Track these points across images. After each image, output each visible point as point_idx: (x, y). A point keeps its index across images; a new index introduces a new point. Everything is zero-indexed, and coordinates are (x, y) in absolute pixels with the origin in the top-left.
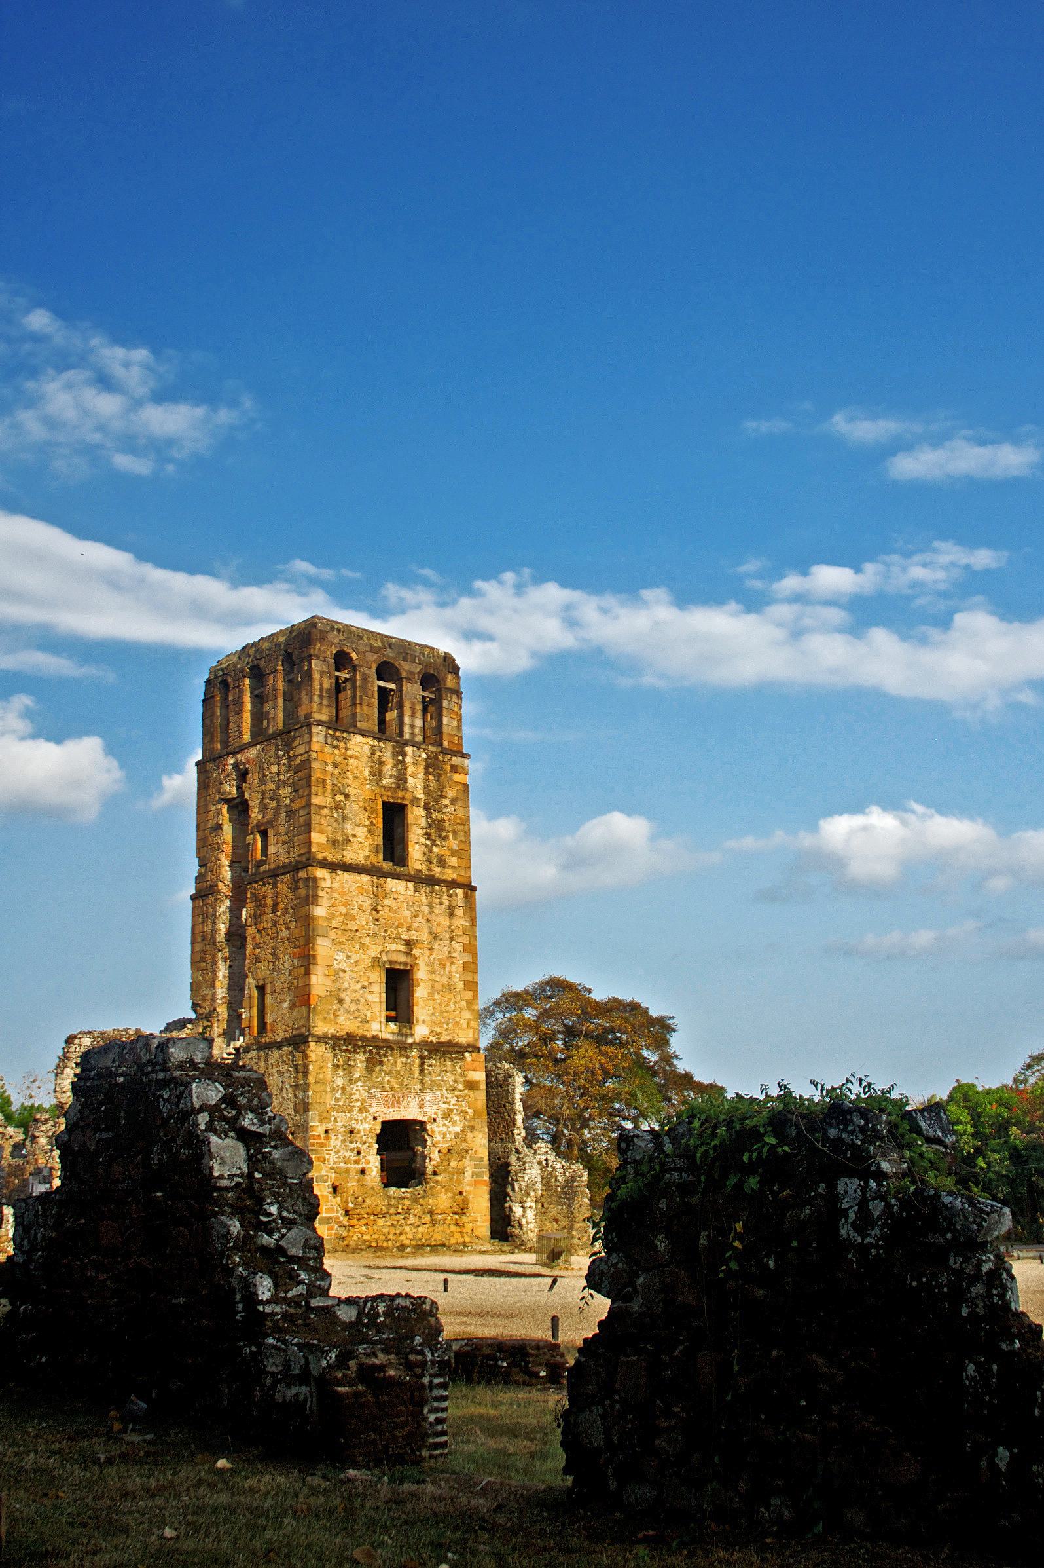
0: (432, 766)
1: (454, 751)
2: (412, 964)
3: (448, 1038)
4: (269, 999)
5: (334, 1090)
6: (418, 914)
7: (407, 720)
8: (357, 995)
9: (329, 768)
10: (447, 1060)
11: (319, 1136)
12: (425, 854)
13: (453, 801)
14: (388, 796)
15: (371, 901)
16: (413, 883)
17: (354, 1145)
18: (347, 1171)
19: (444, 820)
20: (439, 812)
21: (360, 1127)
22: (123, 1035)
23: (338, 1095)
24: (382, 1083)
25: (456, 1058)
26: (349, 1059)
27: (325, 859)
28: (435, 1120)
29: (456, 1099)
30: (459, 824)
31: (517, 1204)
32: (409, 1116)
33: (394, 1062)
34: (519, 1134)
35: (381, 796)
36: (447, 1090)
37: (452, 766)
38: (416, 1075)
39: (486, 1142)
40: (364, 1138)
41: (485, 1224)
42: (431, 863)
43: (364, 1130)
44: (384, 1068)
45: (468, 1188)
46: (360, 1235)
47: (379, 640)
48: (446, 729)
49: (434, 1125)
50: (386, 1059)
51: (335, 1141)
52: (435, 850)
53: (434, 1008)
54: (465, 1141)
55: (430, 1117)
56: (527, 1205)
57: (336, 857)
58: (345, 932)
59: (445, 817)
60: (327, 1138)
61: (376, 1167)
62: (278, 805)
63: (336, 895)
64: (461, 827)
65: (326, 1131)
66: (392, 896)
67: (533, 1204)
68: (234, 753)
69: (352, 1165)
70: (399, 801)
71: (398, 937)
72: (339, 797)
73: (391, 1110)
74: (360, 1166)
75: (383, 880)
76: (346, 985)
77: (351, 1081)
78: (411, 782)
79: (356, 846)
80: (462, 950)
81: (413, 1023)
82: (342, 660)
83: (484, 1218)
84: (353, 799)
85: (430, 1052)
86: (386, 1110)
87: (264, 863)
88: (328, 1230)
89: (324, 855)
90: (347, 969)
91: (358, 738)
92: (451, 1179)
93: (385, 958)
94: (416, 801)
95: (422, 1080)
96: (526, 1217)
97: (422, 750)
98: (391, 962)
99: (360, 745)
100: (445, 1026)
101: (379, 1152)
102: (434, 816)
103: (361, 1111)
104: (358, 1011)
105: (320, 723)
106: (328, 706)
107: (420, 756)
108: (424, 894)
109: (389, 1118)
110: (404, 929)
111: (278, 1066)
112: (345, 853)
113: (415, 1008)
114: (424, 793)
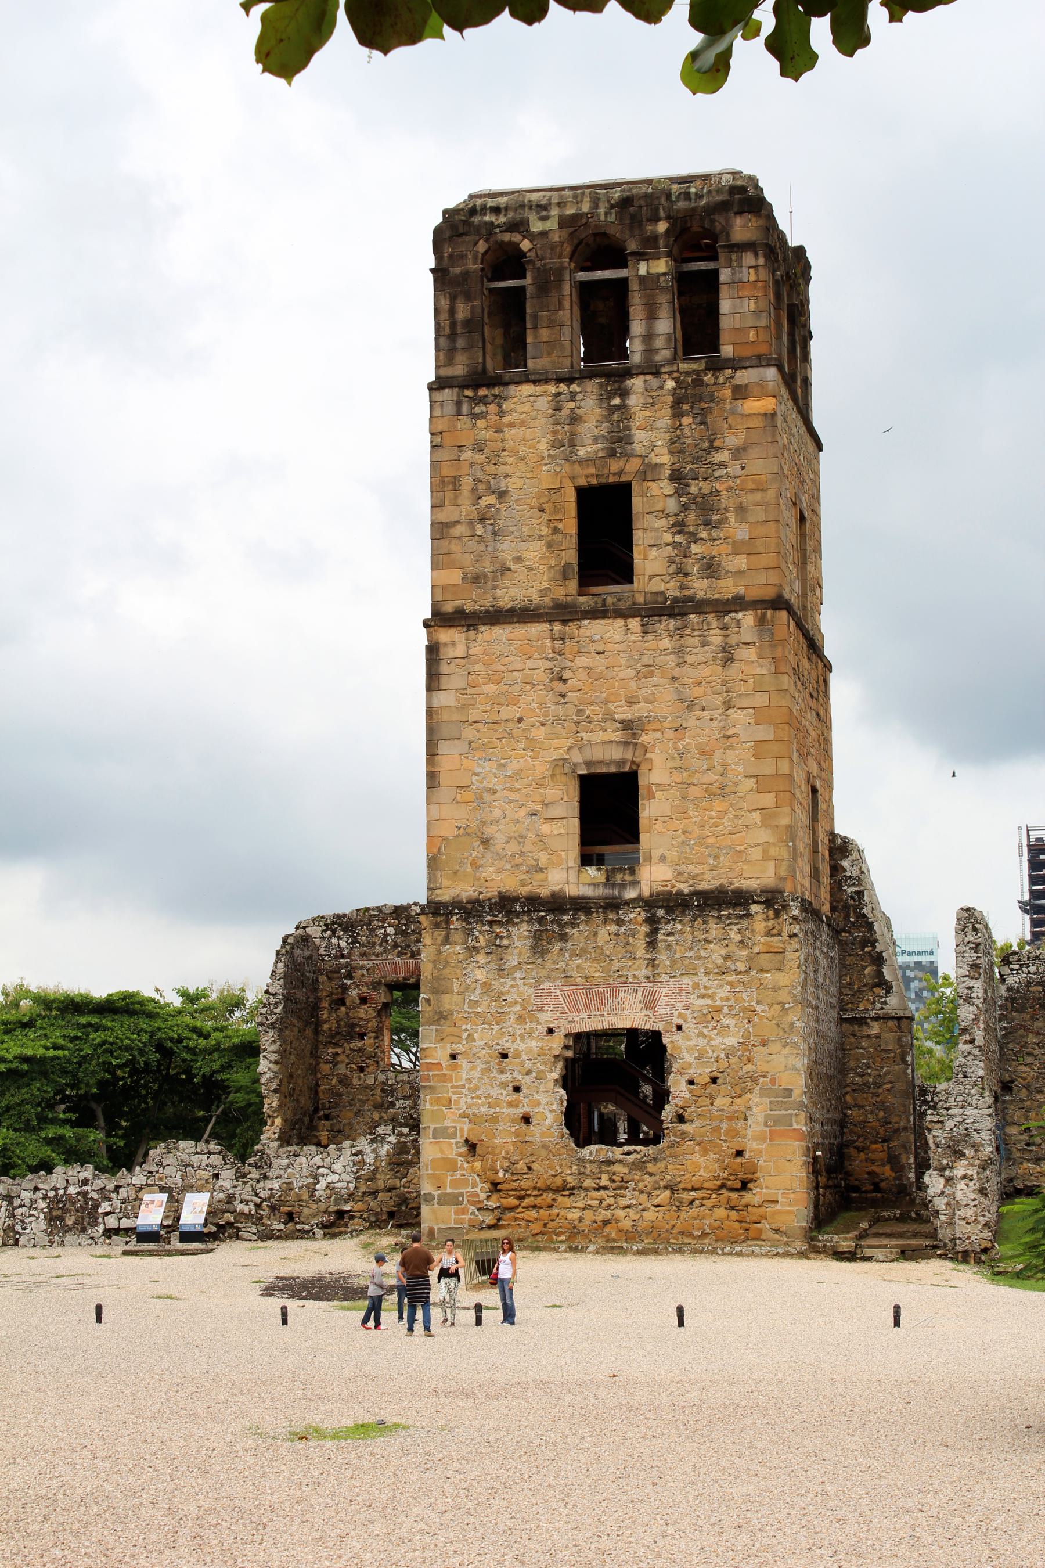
1: (742, 359)
2: (637, 760)
6: (652, 672)
7: (637, 327)
9: (467, 455)
10: (711, 920)
11: (440, 1064)
13: (738, 452)
14: (587, 476)
15: (550, 665)
16: (638, 619)
18: (494, 1119)
20: (705, 479)
21: (522, 1047)
22: (375, 916)
25: (729, 916)
28: (679, 1028)
29: (728, 987)
30: (752, 491)
31: (935, 1173)
32: (623, 1022)
34: (972, 1042)
35: (572, 478)
36: (706, 974)
38: (641, 951)
40: (528, 1065)
41: (795, 1209)
42: (686, 575)
43: (530, 1051)
44: (569, 945)
45: (755, 1145)
46: (523, 1223)
47: (587, 199)
48: (725, 323)
49: (679, 1037)
50: (574, 931)
51: (465, 1070)
53: (685, 832)
56: (959, 1172)
57: (481, 602)
58: (495, 726)
59: (717, 486)
60: (454, 1068)
61: (552, 1111)
63: (478, 667)
64: (758, 497)
65: (453, 1057)
66: (592, 649)
69: (504, 1110)
70: (611, 480)
71: (609, 717)
73: (584, 1015)
74: (520, 1111)
75: (571, 628)
76: (497, 813)
80: (752, 721)
83: (792, 1196)
84: (516, 497)
85: (669, 910)
88: (456, 1213)
89: (457, 603)
90: (498, 788)
91: (527, 389)
92: (716, 1130)
93: (577, 757)
94: (649, 472)
95: (654, 960)
96: (954, 1193)
97: (667, 376)
98: (588, 764)
100: (712, 862)
102: (693, 489)
103: (521, 1019)
104: (522, 854)
106: (469, 348)
107: (661, 388)
108: (665, 634)
109: (578, 1028)
110: (623, 703)
112: (499, 593)
114: (671, 453)
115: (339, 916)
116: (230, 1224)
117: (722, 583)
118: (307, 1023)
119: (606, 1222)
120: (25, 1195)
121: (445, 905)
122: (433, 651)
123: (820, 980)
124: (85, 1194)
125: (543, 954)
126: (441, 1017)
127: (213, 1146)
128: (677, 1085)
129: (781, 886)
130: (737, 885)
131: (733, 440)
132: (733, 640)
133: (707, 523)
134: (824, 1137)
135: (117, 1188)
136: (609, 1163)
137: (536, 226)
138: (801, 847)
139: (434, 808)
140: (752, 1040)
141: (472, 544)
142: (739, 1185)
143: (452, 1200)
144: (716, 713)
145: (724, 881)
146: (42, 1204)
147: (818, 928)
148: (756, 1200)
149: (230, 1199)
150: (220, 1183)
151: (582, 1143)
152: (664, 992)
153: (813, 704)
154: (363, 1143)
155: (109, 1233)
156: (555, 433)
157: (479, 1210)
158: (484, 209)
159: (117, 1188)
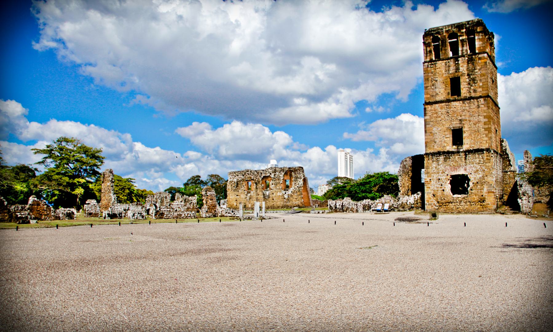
1: (480, 53)
3: (477, 148)
5: (432, 168)
7: (460, 49)
8: (441, 139)
12: (468, 90)
13: (480, 70)
17: (440, 183)
18: (438, 191)
20: (474, 75)
21: (442, 178)
23: (434, 169)
24: (450, 164)
26: (438, 158)
27: (429, 102)
28: (471, 174)
29: (479, 166)
30: (483, 76)
35: (449, 77)
38: (463, 160)
40: (443, 181)
42: (471, 92)
44: (450, 160)
45: (485, 194)
49: (471, 176)
54: (484, 179)
55: (469, 173)
59: (476, 76)
60: (430, 182)
65: (430, 180)
67: (527, 198)
71: (457, 119)
73: (453, 172)
74: (442, 189)
75: (449, 104)
78: (461, 68)
81: (463, 144)
85: (469, 153)
89: (429, 101)
91: (440, 62)
92: (478, 192)
93: (451, 127)
94: (463, 75)
98: (453, 127)
100: (476, 144)
102: (471, 77)
103: (442, 173)
112: (436, 98)
113: (464, 140)
114: (467, 71)
116: (393, 209)
117: (477, 94)
118: (407, 175)
119: (458, 208)
120: (359, 204)
121: (428, 153)
122: (425, 109)
123: (498, 165)
124: (369, 204)
125: (446, 161)
128: (471, 184)
129: (489, 147)
130: (481, 148)
131: (478, 68)
132: (480, 103)
133: (474, 83)
134: (499, 192)
135: (374, 203)
136: (458, 198)
138: (493, 141)
139: (426, 137)
140: (484, 175)
141: (432, 90)
142: (482, 201)
144: (477, 117)
145: (479, 147)
146: (362, 206)
147: (497, 155)
149: (393, 205)
150: (391, 202)
151: (453, 194)
152: (468, 167)
153: (496, 115)
154: (415, 195)
155: (373, 210)
156: (446, 69)
157: (436, 206)
158: (432, 31)
159: (374, 203)
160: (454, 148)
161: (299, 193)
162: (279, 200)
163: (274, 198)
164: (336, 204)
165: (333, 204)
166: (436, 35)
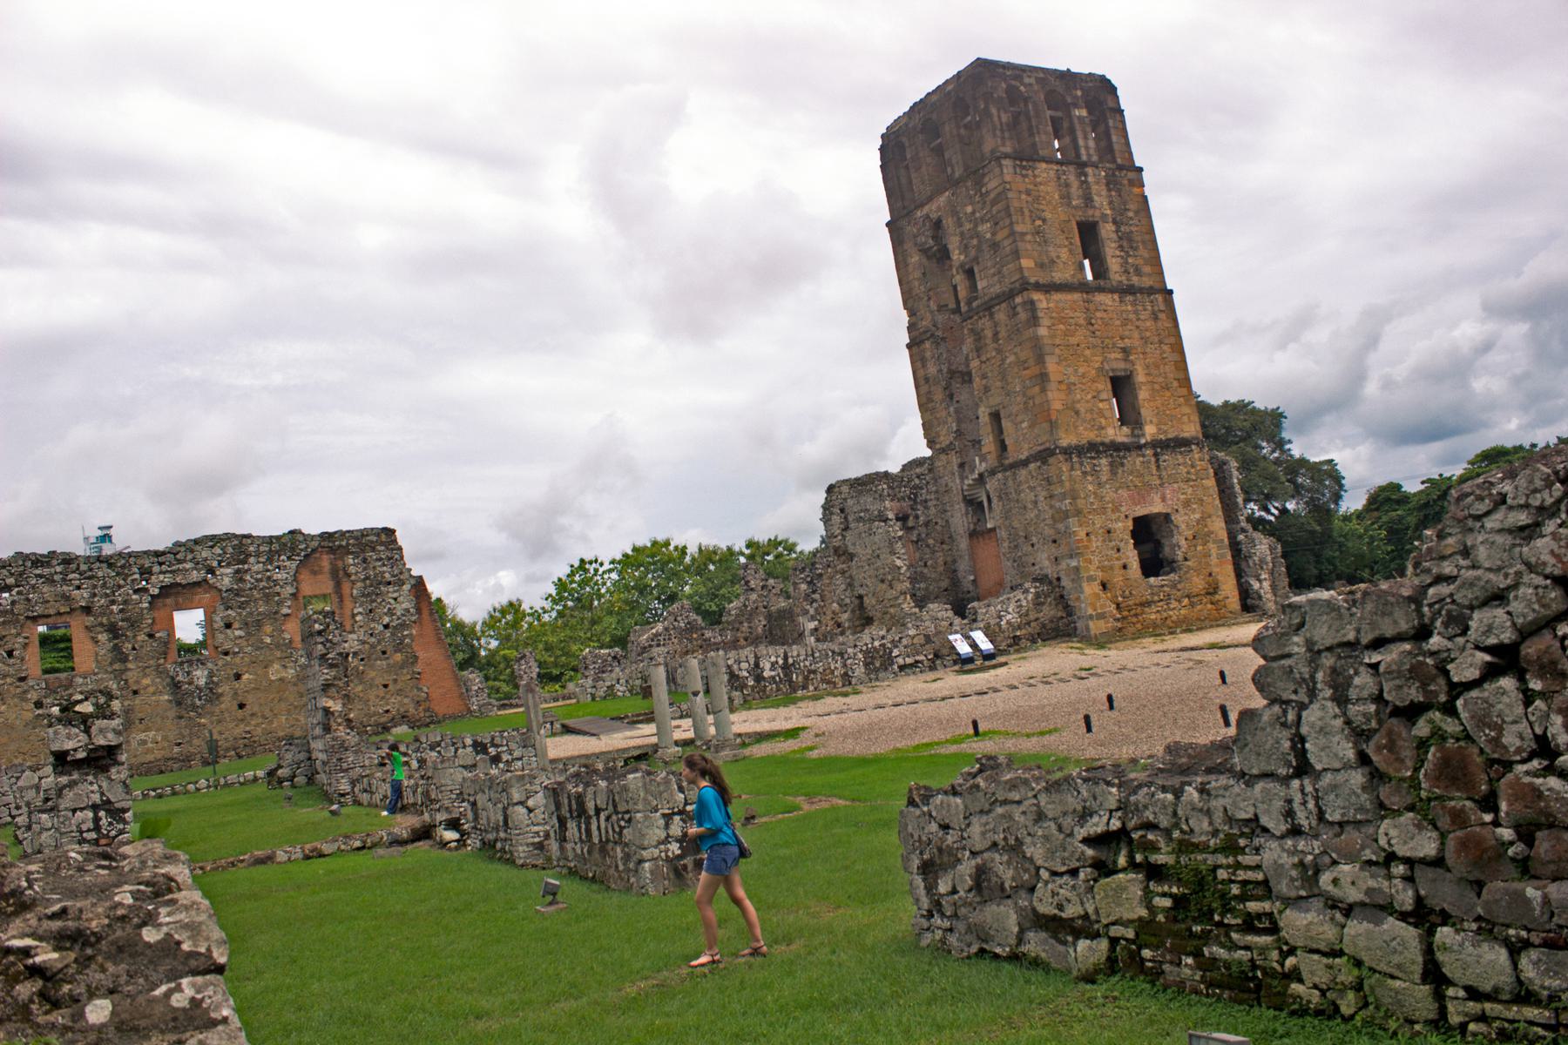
0: (1111, 183)
4: (1005, 424)
7: (1081, 142)
9: (1023, 196)
13: (1137, 213)
18: (1111, 568)
19: (1132, 232)
33: (1135, 461)
37: (1129, 180)
39: (1223, 525)
51: (1096, 543)
52: (1130, 260)
56: (1263, 577)
60: (1089, 541)
62: (979, 242)
65: (1087, 535)
68: (922, 205)
72: (1039, 223)
75: (1090, 297)
76: (1078, 396)
77: (1100, 485)
78: (1096, 198)
79: (1061, 266)
82: (1013, 97)
86: (1133, 507)
87: (976, 298)
91: (1044, 165)
93: (1107, 367)
94: (1104, 216)
98: (1113, 370)
99: (1044, 171)
101: (1136, 545)
105: (1007, 156)
106: (1011, 138)
111: (1027, 482)
115: (857, 479)
126: (1078, 513)
127: (949, 606)
137: (1027, 80)
141: (1035, 246)
143: (1101, 616)
146: (860, 656)
148: (1220, 598)
154: (1019, 595)
155: (902, 668)
160: (1120, 434)
161: (398, 657)
162: (283, 705)
163: (250, 700)
164: (757, 665)
165: (744, 665)
166: (1013, 82)
